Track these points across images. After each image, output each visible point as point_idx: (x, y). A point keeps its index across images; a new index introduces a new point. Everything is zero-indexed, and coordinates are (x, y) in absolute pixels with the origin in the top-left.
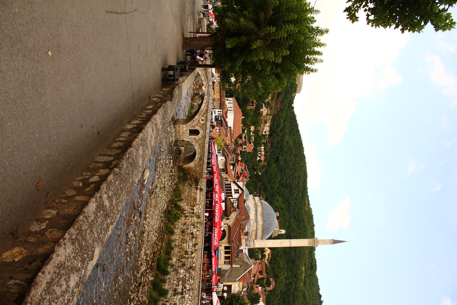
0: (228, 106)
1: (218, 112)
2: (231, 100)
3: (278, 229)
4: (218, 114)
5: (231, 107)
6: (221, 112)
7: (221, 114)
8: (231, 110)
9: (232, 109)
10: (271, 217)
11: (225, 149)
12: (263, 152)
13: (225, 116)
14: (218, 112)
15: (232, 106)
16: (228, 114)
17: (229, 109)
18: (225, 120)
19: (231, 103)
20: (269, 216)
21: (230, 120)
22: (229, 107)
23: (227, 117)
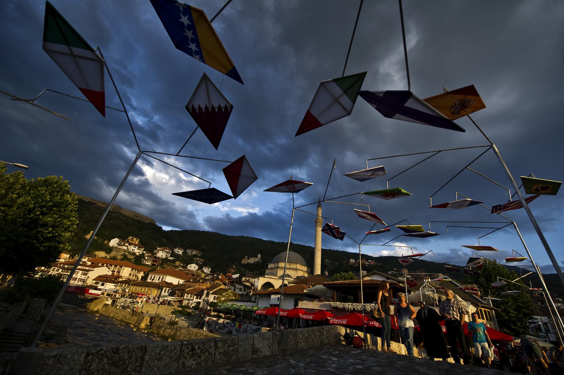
0: (157, 281)
1: (165, 292)
2: (151, 277)
3: (258, 258)
4: (168, 292)
5: (159, 278)
6: (166, 289)
7: (169, 290)
8: (163, 278)
9: (161, 277)
10: (291, 255)
11: (214, 291)
12: (197, 259)
13: (169, 285)
14: (165, 292)
15: (158, 276)
16: (166, 281)
17: (160, 281)
18: (176, 286)
19: (154, 277)
20: (291, 258)
21: (174, 281)
22: (159, 280)
23: (171, 284)
